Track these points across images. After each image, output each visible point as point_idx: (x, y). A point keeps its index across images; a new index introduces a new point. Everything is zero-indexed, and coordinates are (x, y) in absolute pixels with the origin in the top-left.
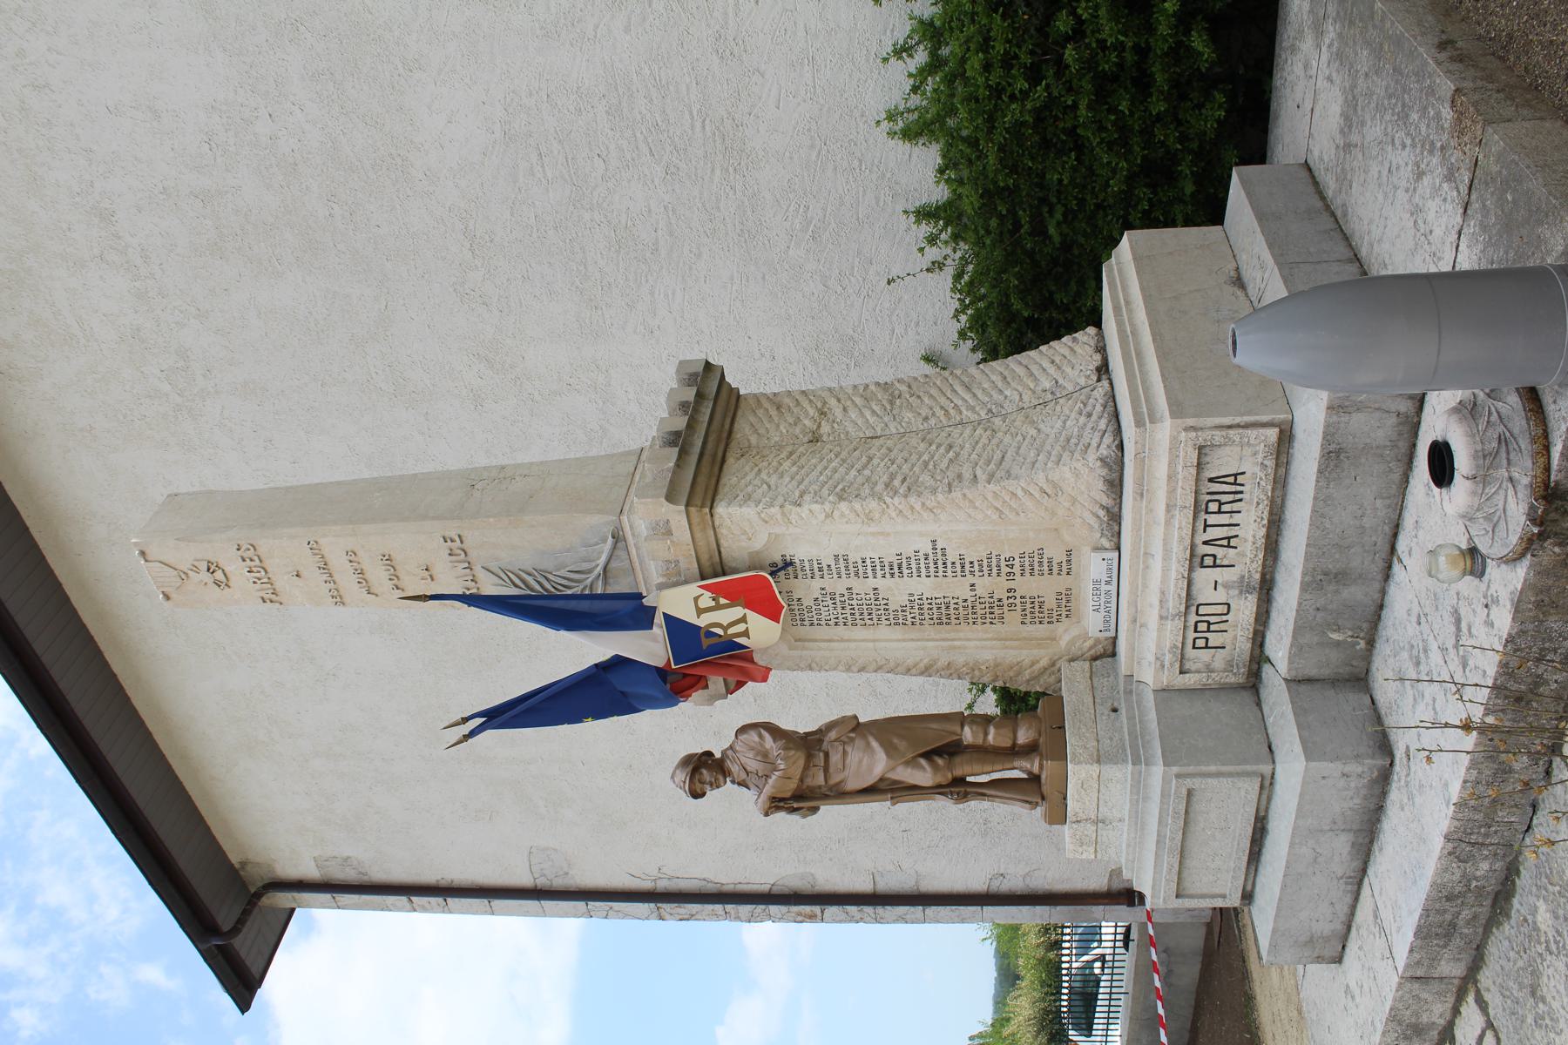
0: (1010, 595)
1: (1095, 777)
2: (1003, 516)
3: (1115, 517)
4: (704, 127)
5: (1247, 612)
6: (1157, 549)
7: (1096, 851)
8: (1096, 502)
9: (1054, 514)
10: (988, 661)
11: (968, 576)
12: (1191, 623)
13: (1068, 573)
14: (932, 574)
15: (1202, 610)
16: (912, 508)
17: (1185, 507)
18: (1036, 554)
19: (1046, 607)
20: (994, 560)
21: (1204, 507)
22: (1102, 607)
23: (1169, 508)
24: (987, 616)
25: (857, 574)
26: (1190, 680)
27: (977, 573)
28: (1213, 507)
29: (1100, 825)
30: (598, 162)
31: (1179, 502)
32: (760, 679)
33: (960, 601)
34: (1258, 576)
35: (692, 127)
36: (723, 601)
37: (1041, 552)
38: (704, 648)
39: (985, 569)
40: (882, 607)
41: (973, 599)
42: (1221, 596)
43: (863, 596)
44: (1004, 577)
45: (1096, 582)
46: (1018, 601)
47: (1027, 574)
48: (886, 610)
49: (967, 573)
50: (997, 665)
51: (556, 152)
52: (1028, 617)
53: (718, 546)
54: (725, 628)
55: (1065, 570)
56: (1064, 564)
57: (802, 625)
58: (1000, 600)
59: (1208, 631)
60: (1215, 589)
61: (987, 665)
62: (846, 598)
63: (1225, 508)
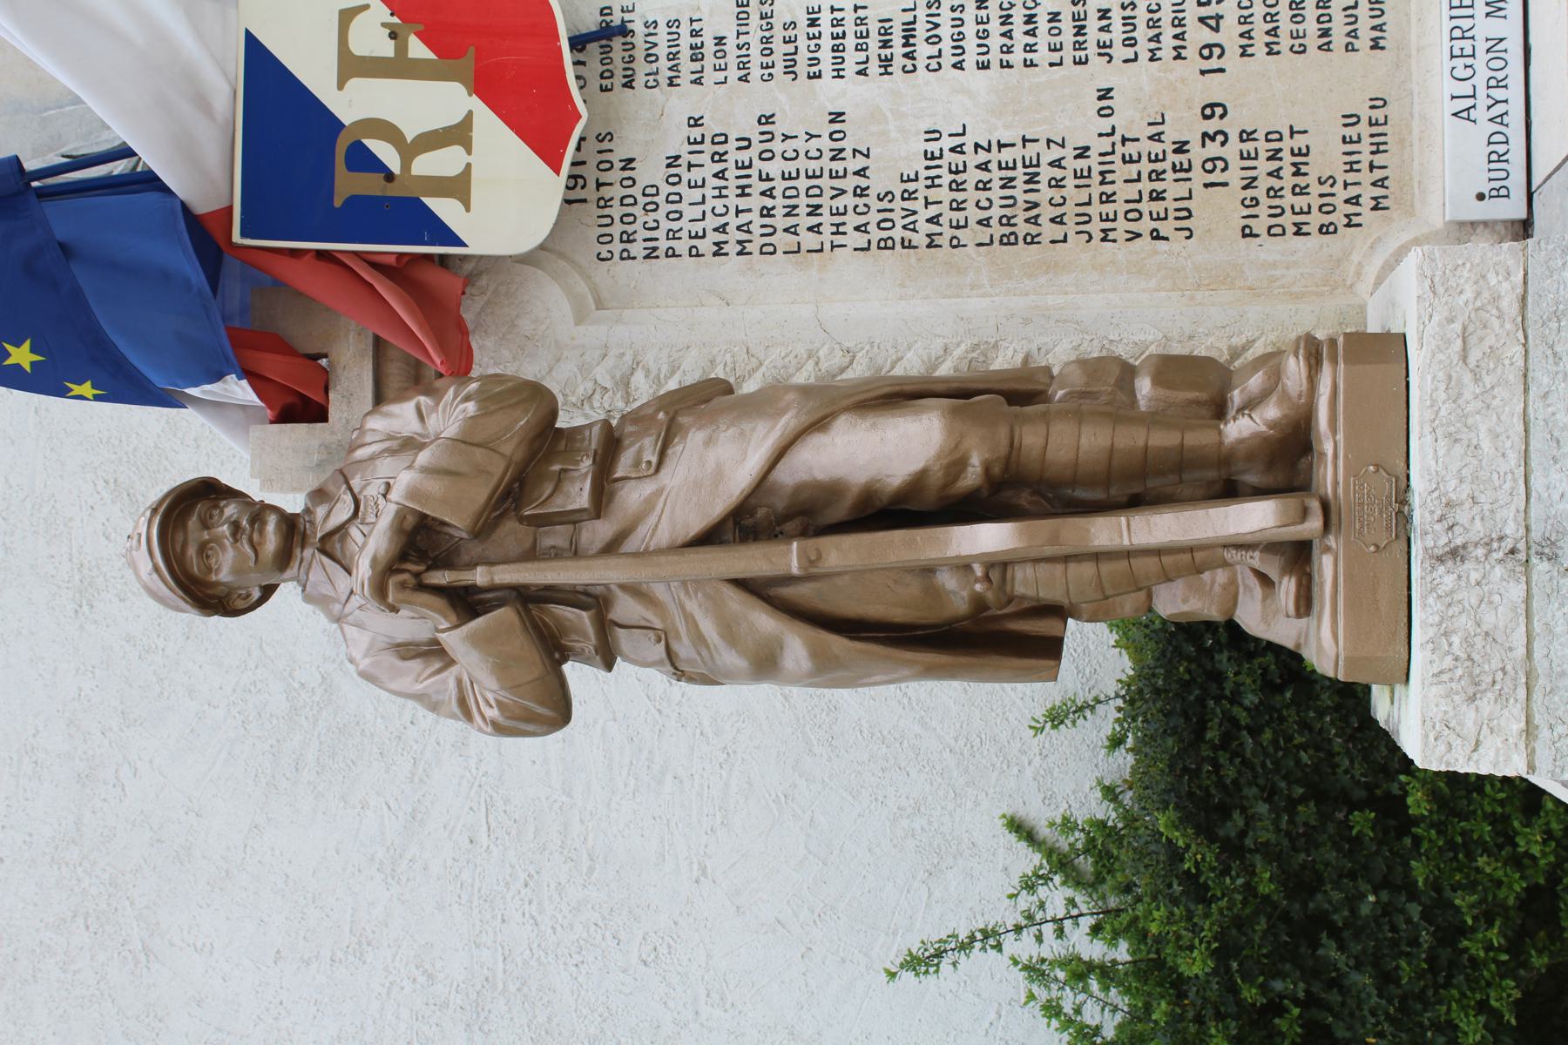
0: (1212, 126)
1: (1509, 304)
7: (1530, 731)
11: (1097, 62)
13: (1376, 46)
14: (995, 56)
19: (1314, 170)
22: (1482, 102)
24: (1145, 206)
25: (790, 70)
27: (1120, 52)
29: (1541, 567)
33: (1069, 152)
36: (418, 49)
38: (338, 202)
39: (1142, 33)
40: (850, 183)
43: (799, 144)
44: (1194, 62)
46: (1232, 151)
47: (1259, 49)
48: (860, 192)
49: (1092, 49)
52: (1262, 210)
54: (409, 151)
55: (1365, 35)
57: (627, 257)
58: (1181, 148)
62: (753, 152)
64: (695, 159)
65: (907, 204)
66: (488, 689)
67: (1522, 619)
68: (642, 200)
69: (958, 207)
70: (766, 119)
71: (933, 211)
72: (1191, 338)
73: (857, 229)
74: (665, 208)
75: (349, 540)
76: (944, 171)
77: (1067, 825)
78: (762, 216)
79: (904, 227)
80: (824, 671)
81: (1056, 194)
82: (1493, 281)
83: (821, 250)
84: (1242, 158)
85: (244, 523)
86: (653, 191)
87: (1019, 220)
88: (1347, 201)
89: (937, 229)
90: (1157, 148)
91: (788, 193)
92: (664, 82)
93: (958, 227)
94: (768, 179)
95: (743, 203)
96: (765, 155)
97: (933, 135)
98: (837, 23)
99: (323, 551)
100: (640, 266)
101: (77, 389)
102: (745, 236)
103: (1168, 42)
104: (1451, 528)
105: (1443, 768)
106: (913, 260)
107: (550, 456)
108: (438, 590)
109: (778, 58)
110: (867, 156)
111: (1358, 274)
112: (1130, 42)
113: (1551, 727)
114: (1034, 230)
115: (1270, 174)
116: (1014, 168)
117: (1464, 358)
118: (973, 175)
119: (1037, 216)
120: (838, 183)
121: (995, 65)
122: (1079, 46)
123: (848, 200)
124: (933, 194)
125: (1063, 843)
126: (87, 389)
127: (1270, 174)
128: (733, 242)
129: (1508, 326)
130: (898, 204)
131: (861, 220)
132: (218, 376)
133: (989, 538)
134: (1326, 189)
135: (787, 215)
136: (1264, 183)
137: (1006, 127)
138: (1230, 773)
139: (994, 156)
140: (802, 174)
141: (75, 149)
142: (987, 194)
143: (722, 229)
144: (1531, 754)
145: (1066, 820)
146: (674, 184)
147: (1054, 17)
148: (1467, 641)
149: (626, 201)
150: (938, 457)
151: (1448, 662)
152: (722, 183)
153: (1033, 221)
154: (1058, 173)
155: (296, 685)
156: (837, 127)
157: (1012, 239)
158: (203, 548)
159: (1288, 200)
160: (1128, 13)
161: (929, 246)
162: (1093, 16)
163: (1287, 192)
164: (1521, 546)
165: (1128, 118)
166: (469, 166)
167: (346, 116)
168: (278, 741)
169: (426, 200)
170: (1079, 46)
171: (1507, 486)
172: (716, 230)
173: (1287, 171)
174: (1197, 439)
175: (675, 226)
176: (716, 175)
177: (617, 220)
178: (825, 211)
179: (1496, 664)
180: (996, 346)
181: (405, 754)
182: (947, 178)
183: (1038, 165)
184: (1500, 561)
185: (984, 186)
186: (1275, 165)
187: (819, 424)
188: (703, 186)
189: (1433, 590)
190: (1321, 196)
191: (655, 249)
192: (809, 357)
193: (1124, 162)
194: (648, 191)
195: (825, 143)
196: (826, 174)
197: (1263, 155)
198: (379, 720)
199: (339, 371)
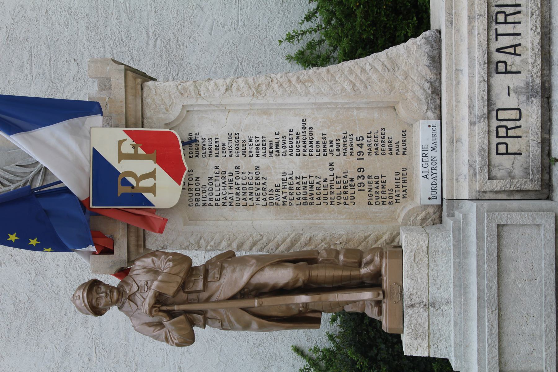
0: (360, 174)
1: (425, 248)
2: (356, 88)
3: (436, 92)
4: (155, 45)
5: (534, 116)
6: (464, 65)
7: (429, 346)
8: (423, 77)
9: (392, 88)
10: (341, 236)
11: (329, 155)
12: (494, 129)
13: (404, 154)
14: (301, 153)
15: (501, 115)
16: (290, 81)
17: (481, 15)
18: (379, 134)
19: (388, 186)
20: (348, 139)
21: (494, 18)
22: (430, 173)
23: (471, 19)
24: (342, 195)
25: (244, 154)
26: (497, 185)
27: (335, 153)
28: (501, 18)
29: (431, 309)
30: (74, 65)
31: (477, 12)
32: (158, 230)
33: (322, 180)
34: (538, 81)
35: (147, 44)
36: (140, 151)
37: (383, 131)
38: (119, 195)
39: (341, 148)
40: (261, 186)
41: (331, 178)
42: (512, 101)
43: (247, 175)
44: (356, 156)
45: (425, 148)
46: (366, 181)
47: (373, 153)
48: (264, 189)
49: (328, 152)
50: (348, 241)
51: (43, 55)
52: (374, 197)
53: (143, 118)
54: (138, 180)
55: (401, 150)
56: (401, 144)
57: (197, 205)
58: (352, 180)
59: (507, 136)
60: (509, 94)
61: (341, 240)
62: (234, 177)
63: (510, 19)
64: (217, 178)
65: (277, 193)
66: (175, 335)
67: (427, 321)
68: (201, 189)
69: (291, 194)
70: (237, 168)
71: (284, 195)
72: (354, 233)
73: (263, 199)
74: (208, 192)
75: (136, 297)
76: (287, 184)
77: (316, 350)
78: (236, 195)
79: (276, 199)
80: (261, 328)
81: (318, 192)
82: (421, 243)
83: (253, 205)
84: (368, 183)
85: (108, 292)
86: (205, 187)
87: (308, 198)
88: (396, 196)
89: (285, 200)
90: (345, 180)
91: (243, 189)
92: (208, 156)
93: (291, 200)
94: (238, 185)
95: (231, 191)
96: (237, 178)
97: (284, 174)
98: (257, 141)
99: (129, 299)
100: (201, 208)
101: (46, 250)
102: (231, 201)
103: (348, 150)
104: (411, 300)
105: (409, 355)
106: (279, 208)
107: (191, 275)
108: (164, 311)
109: (240, 150)
110: (266, 179)
111: (399, 216)
112: (338, 150)
113: (434, 345)
114: (312, 201)
115: (376, 188)
116: (307, 184)
117: (414, 261)
118: (295, 186)
119: (313, 197)
120: (258, 186)
121: (301, 155)
122: (324, 151)
123: (260, 191)
124: (284, 190)
125: (315, 356)
126: (50, 249)
127: (376, 188)
128: (228, 202)
129: (424, 253)
130: (274, 193)
131: (264, 197)
132: (87, 246)
133: (303, 299)
134: (390, 192)
135: (243, 195)
136: (374, 190)
137: (304, 172)
138: (372, 334)
139: (301, 180)
140: (248, 184)
141: (21, 163)
142: (299, 191)
143: (225, 198)
144: (429, 351)
145: (315, 348)
146: (211, 185)
147: (318, 142)
148: (415, 326)
149: (197, 189)
150: (292, 279)
151: (411, 330)
152: (225, 185)
153: (312, 199)
154: (319, 186)
155: (18, 301)
156: (257, 171)
157: (306, 203)
158: (97, 299)
159: (380, 195)
160: (338, 142)
161: (283, 205)
162: (328, 142)
163: (380, 193)
164: (427, 304)
165: (338, 171)
166: (155, 184)
167: (121, 170)
168: (10, 323)
169: (143, 193)
170: (324, 151)
171: (424, 290)
172: (223, 198)
173: (380, 187)
174: (354, 273)
175: (211, 197)
176: (223, 183)
177: (194, 195)
178: (254, 194)
179: (421, 331)
180: (302, 234)
181: (62, 327)
182: (288, 186)
183: (313, 183)
184: (422, 307)
185: (298, 189)
186: (377, 185)
187: (262, 269)
188: (219, 186)
189: (407, 314)
190: (389, 194)
191: (205, 203)
192: (251, 236)
193: (337, 183)
194: (203, 187)
195: (254, 175)
196: (254, 184)
197: (374, 182)
198: (52, 314)
199: (117, 240)
